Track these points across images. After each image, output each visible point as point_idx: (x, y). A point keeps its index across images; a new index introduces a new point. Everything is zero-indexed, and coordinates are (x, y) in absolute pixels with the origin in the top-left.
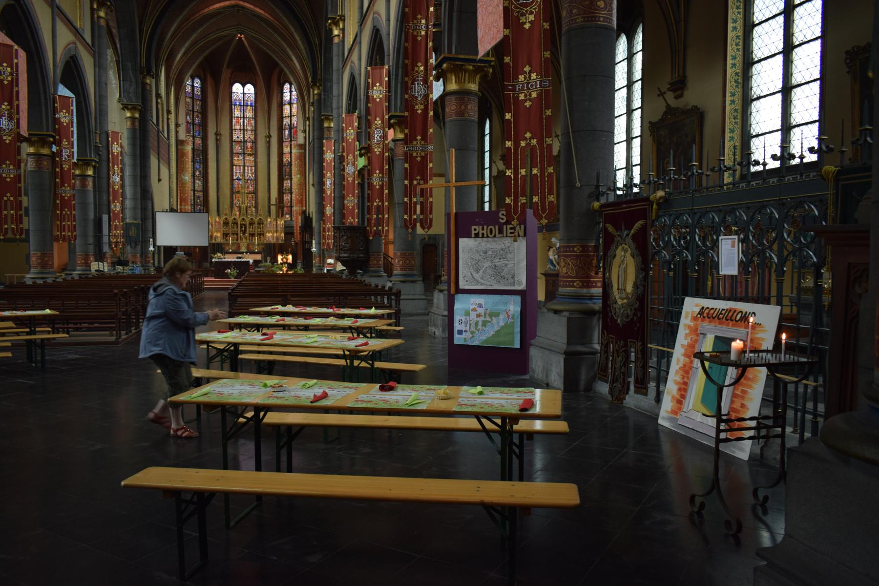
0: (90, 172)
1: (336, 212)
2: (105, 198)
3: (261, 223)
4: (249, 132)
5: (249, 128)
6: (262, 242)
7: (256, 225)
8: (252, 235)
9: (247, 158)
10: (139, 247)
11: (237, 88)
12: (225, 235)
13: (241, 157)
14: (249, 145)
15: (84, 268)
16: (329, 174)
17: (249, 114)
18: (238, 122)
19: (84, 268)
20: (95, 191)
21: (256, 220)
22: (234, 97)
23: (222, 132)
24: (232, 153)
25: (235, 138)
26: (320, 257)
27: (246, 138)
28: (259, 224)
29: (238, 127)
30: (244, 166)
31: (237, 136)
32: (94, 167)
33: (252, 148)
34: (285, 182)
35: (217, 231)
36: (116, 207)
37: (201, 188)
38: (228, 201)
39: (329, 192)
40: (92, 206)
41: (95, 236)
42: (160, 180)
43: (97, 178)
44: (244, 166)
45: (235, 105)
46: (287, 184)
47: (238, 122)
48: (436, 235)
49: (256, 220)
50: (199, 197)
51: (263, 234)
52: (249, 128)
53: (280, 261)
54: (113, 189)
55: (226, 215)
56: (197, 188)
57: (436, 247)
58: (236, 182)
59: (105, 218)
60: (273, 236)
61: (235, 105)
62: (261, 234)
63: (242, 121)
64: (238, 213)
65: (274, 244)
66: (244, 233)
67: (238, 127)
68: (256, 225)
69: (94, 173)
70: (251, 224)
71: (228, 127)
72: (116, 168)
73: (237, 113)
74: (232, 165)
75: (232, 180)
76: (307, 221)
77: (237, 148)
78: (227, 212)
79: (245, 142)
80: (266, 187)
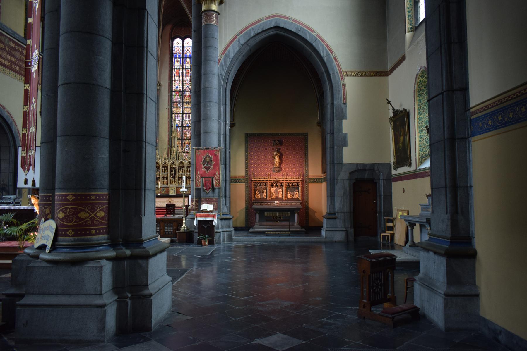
4: (188, 82)
5: (188, 78)
7: (185, 169)
9: (185, 106)
11: (178, 42)
13: (180, 106)
14: (187, 93)
17: (188, 65)
18: (177, 73)
22: (175, 50)
23: (162, 83)
24: (171, 102)
25: (174, 88)
27: (185, 87)
29: (177, 78)
30: (182, 114)
31: (177, 86)
33: (189, 96)
44: (182, 114)
45: (176, 58)
47: (177, 73)
48: (374, 165)
52: (188, 78)
57: (376, 183)
61: (176, 58)
63: (181, 71)
66: (174, 177)
67: (177, 78)
68: (185, 169)
70: (181, 167)
71: (167, 77)
73: (177, 65)
74: (171, 113)
77: (176, 98)
79: (183, 91)
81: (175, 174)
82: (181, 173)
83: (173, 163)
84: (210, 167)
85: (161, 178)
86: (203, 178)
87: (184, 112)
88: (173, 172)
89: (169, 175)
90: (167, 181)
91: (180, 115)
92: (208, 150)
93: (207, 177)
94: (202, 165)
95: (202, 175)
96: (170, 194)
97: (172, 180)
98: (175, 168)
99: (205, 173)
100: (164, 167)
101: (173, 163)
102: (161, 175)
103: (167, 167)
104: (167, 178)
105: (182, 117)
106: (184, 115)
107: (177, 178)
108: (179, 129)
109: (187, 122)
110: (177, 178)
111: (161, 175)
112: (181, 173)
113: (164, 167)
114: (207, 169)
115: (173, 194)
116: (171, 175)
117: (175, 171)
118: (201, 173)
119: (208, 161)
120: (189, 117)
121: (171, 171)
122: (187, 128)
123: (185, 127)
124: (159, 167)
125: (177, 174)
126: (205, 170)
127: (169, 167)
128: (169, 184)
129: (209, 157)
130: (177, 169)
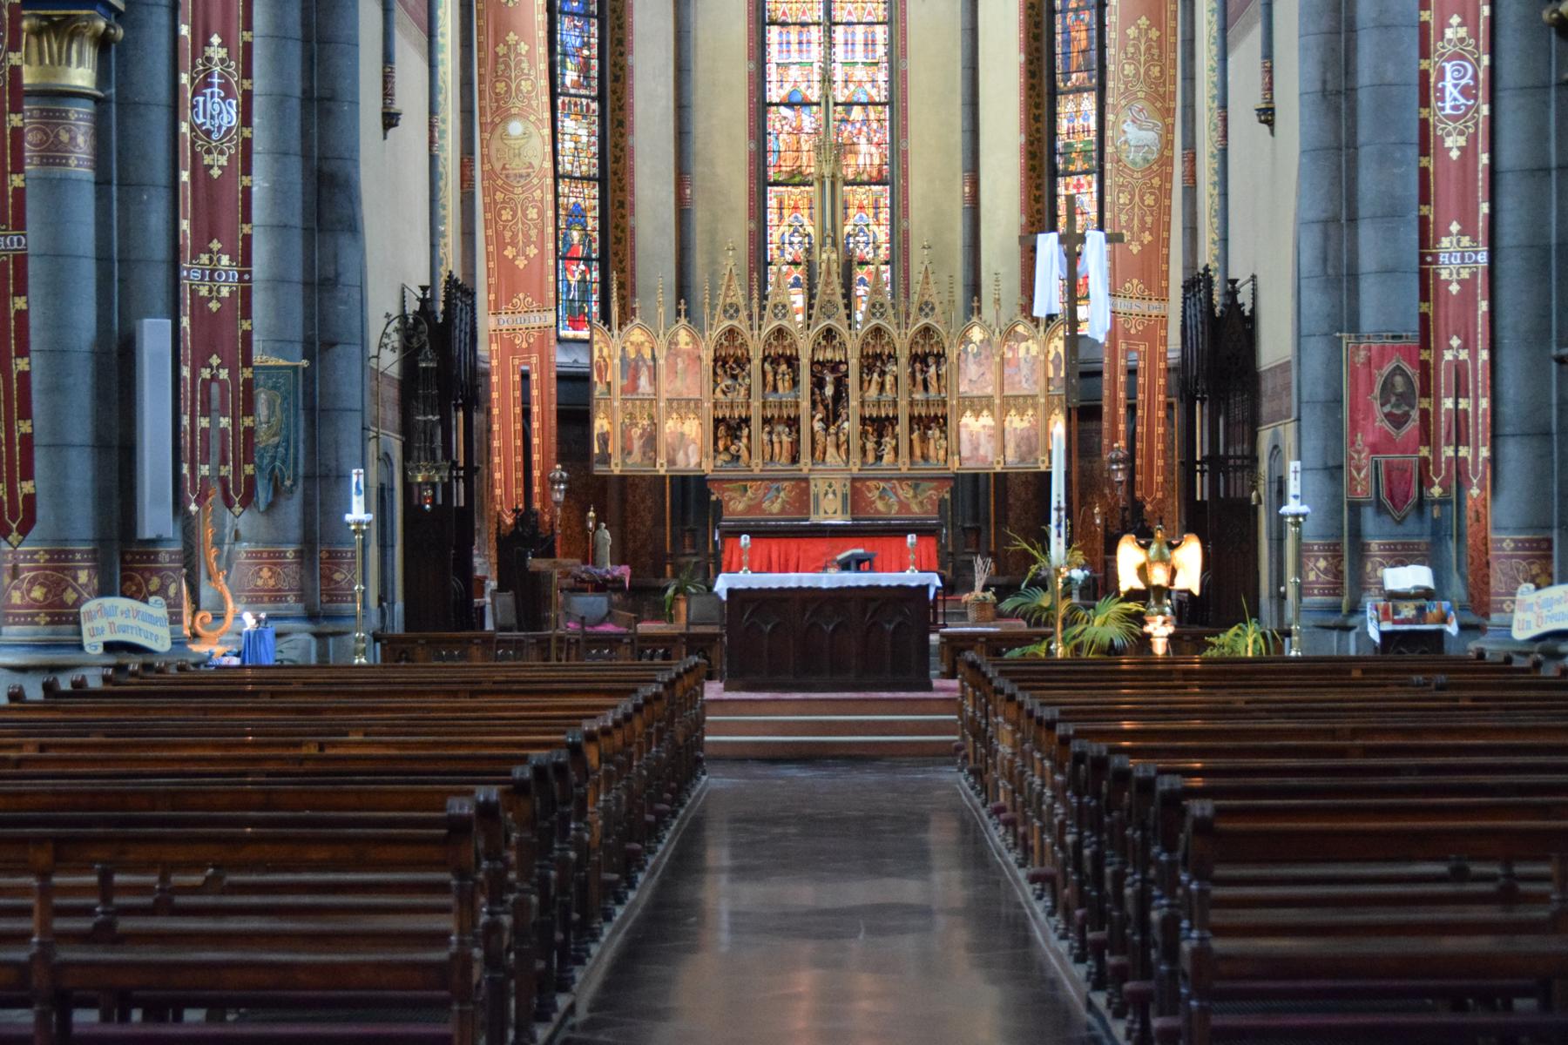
0: (81, 76)
1: (1511, 265)
2: (157, 219)
3: (927, 356)
6: (935, 466)
8: (879, 426)
10: (292, 510)
12: (728, 428)
15: (42, 631)
16: (1455, 31)
19: (42, 631)
20: (102, 183)
21: (901, 341)
26: (1334, 551)
28: (919, 359)
30: (830, 23)
32: (103, 43)
34: (1066, 107)
35: (682, 405)
36: (211, 276)
37: (588, 164)
38: (738, 230)
39: (1454, 144)
40: (87, 270)
41: (101, 444)
42: (390, 120)
43: (115, 107)
44: (830, 23)
46: (1075, 116)
49: (901, 341)
50: (577, 215)
51: (941, 421)
53: (1128, 579)
54: (199, 170)
55: (732, 310)
56: (566, 166)
58: (779, 119)
59: (154, 336)
60: (1001, 433)
62: (932, 421)
64: (798, 299)
65: (1001, 478)
66: (833, 416)
68: (901, 368)
69: (102, 77)
70: (873, 362)
72: (216, 51)
75: (760, 107)
76: (1221, 342)
78: (738, 295)
80: (957, 138)
81: (840, 395)
82: (873, 392)
83: (829, 334)
84: (1406, 416)
85: (756, 423)
86: (1382, 458)
87: (839, 16)
88: (829, 391)
89: (805, 404)
90: (796, 444)
91: (815, 33)
92: (1398, 343)
93: (1396, 457)
94: (1377, 404)
95: (1374, 449)
96: (815, 519)
97: (820, 437)
98: (834, 366)
99: (1389, 438)
100: (775, 361)
101: (829, 334)
102: (756, 403)
103: (792, 361)
104: (793, 423)
105: (830, 44)
106: (839, 32)
107: (850, 426)
108: (808, 120)
109: (860, 73)
110: (850, 426)
111: (756, 403)
112: (873, 392)
113: (775, 361)
114: (1398, 421)
115: (839, 520)
116: (814, 404)
117: (840, 384)
118: (1371, 439)
119: (1400, 390)
120: (870, 44)
121: (818, 383)
122: (857, 113)
123: (849, 105)
124: (742, 362)
125: (854, 403)
126: (1387, 426)
127: (805, 362)
128: (805, 461)
129: (1403, 373)
130: (854, 363)
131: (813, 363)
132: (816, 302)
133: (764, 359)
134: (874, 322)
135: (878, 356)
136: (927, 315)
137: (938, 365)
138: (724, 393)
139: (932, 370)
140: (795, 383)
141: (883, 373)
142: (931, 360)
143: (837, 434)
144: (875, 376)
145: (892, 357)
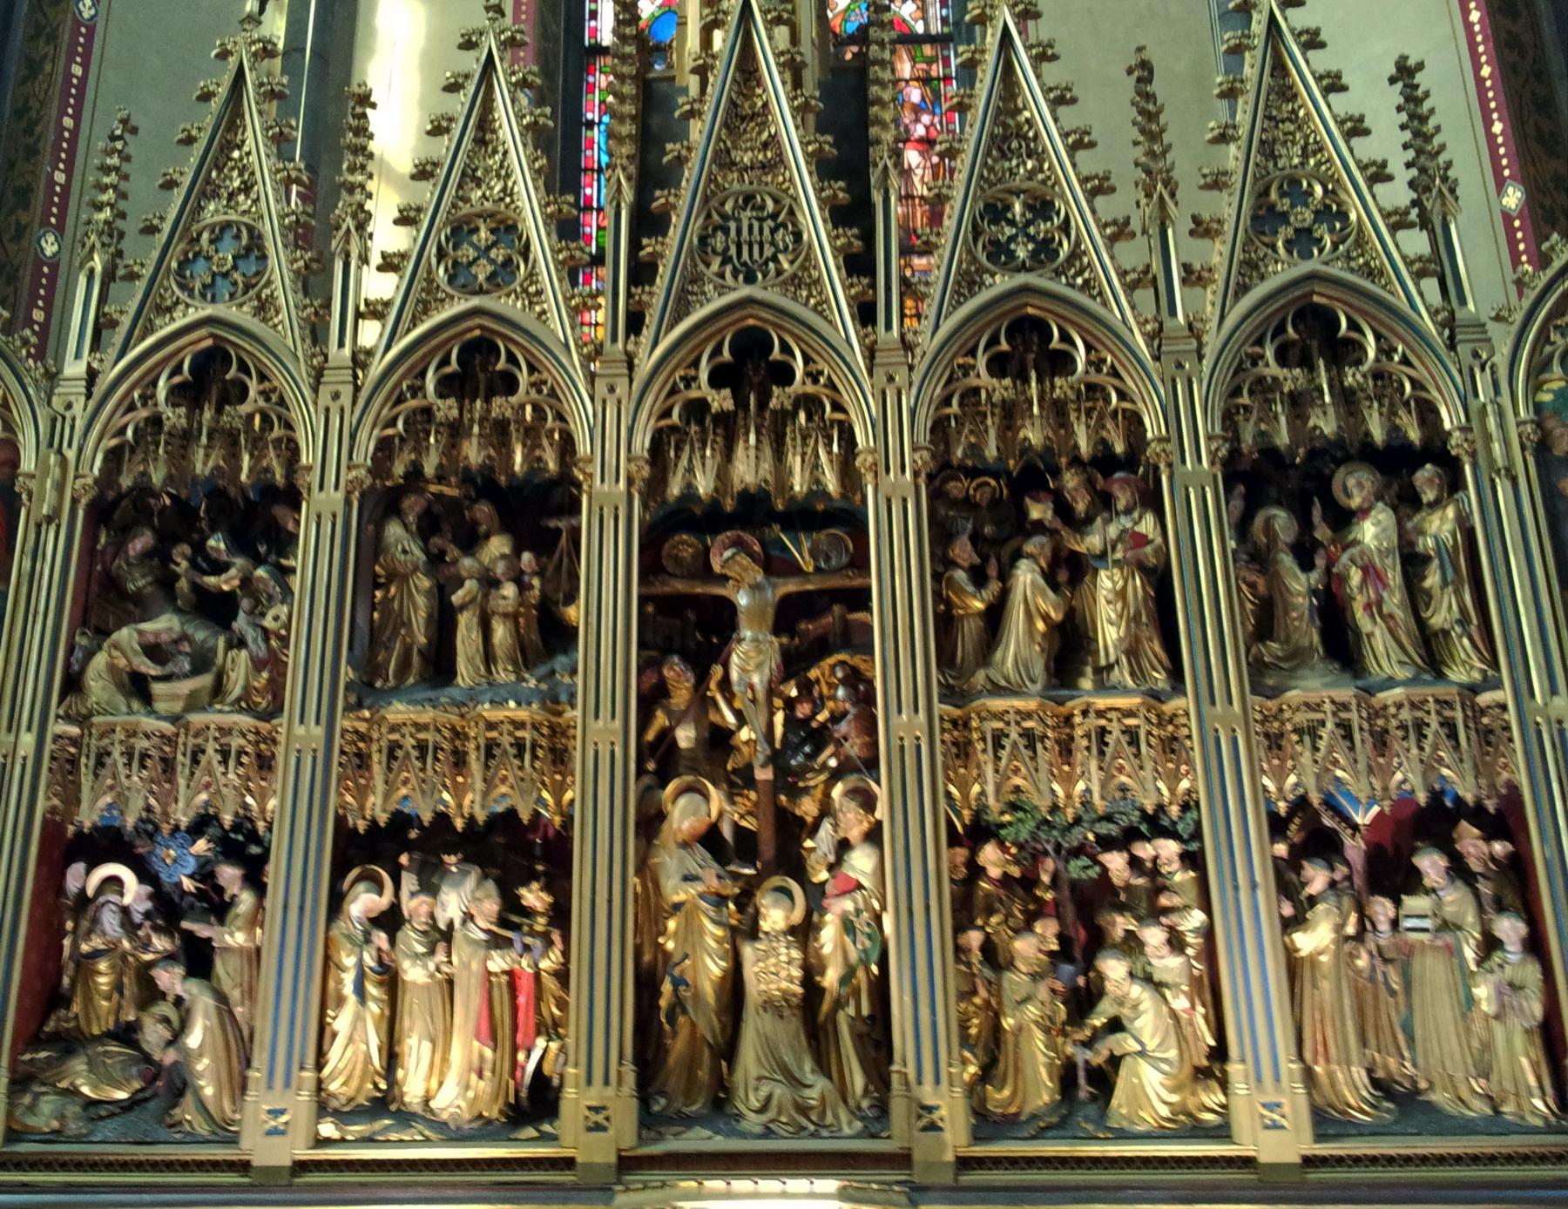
28: (1279, 486)
100: (448, 528)
103: (539, 510)
121: (685, 628)
124: (262, 519)
131: (670, 526)
132: (682, 204)
133: (380, 502)
134: (1001, 283)
135: (1034, 475)
136: (1303, 241)
137: (1407, 502)
138: (137, 687)
139: (1372, 531)
140: (549, 636)
141: (1070, 572)
142: (1355, 486)
143: (803, 933)
144: (1026, 576)
145: (1127, 470)
